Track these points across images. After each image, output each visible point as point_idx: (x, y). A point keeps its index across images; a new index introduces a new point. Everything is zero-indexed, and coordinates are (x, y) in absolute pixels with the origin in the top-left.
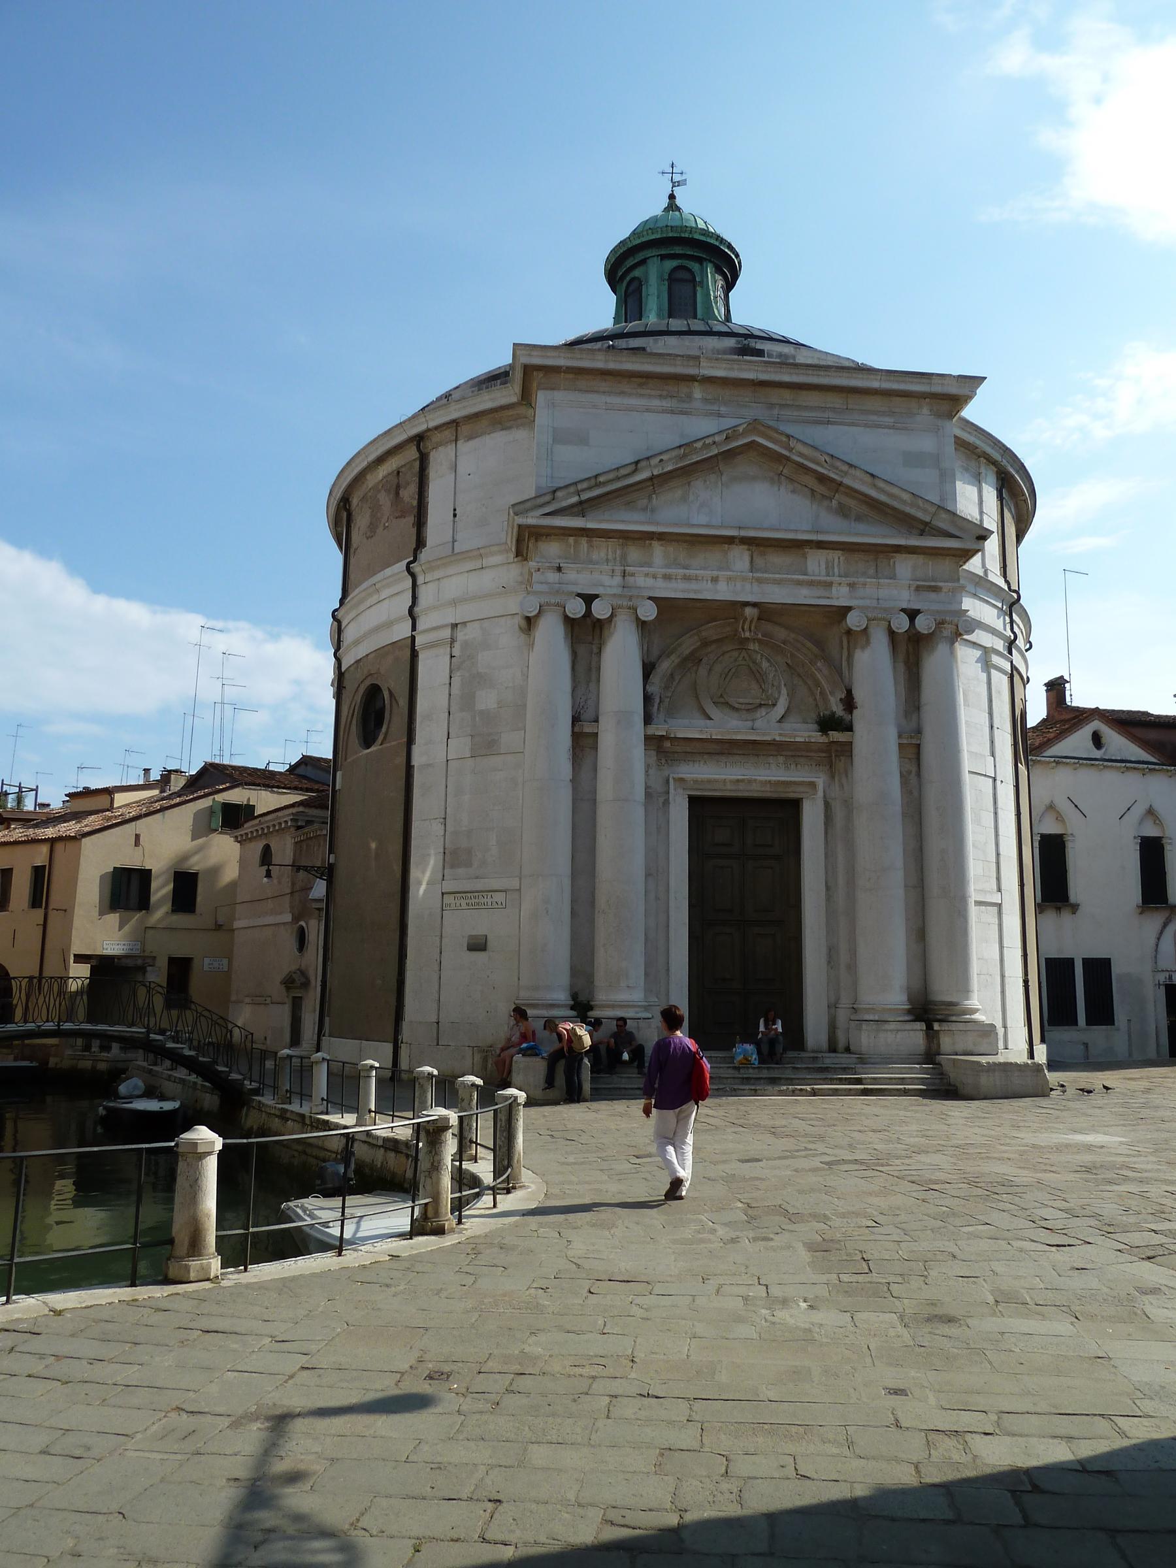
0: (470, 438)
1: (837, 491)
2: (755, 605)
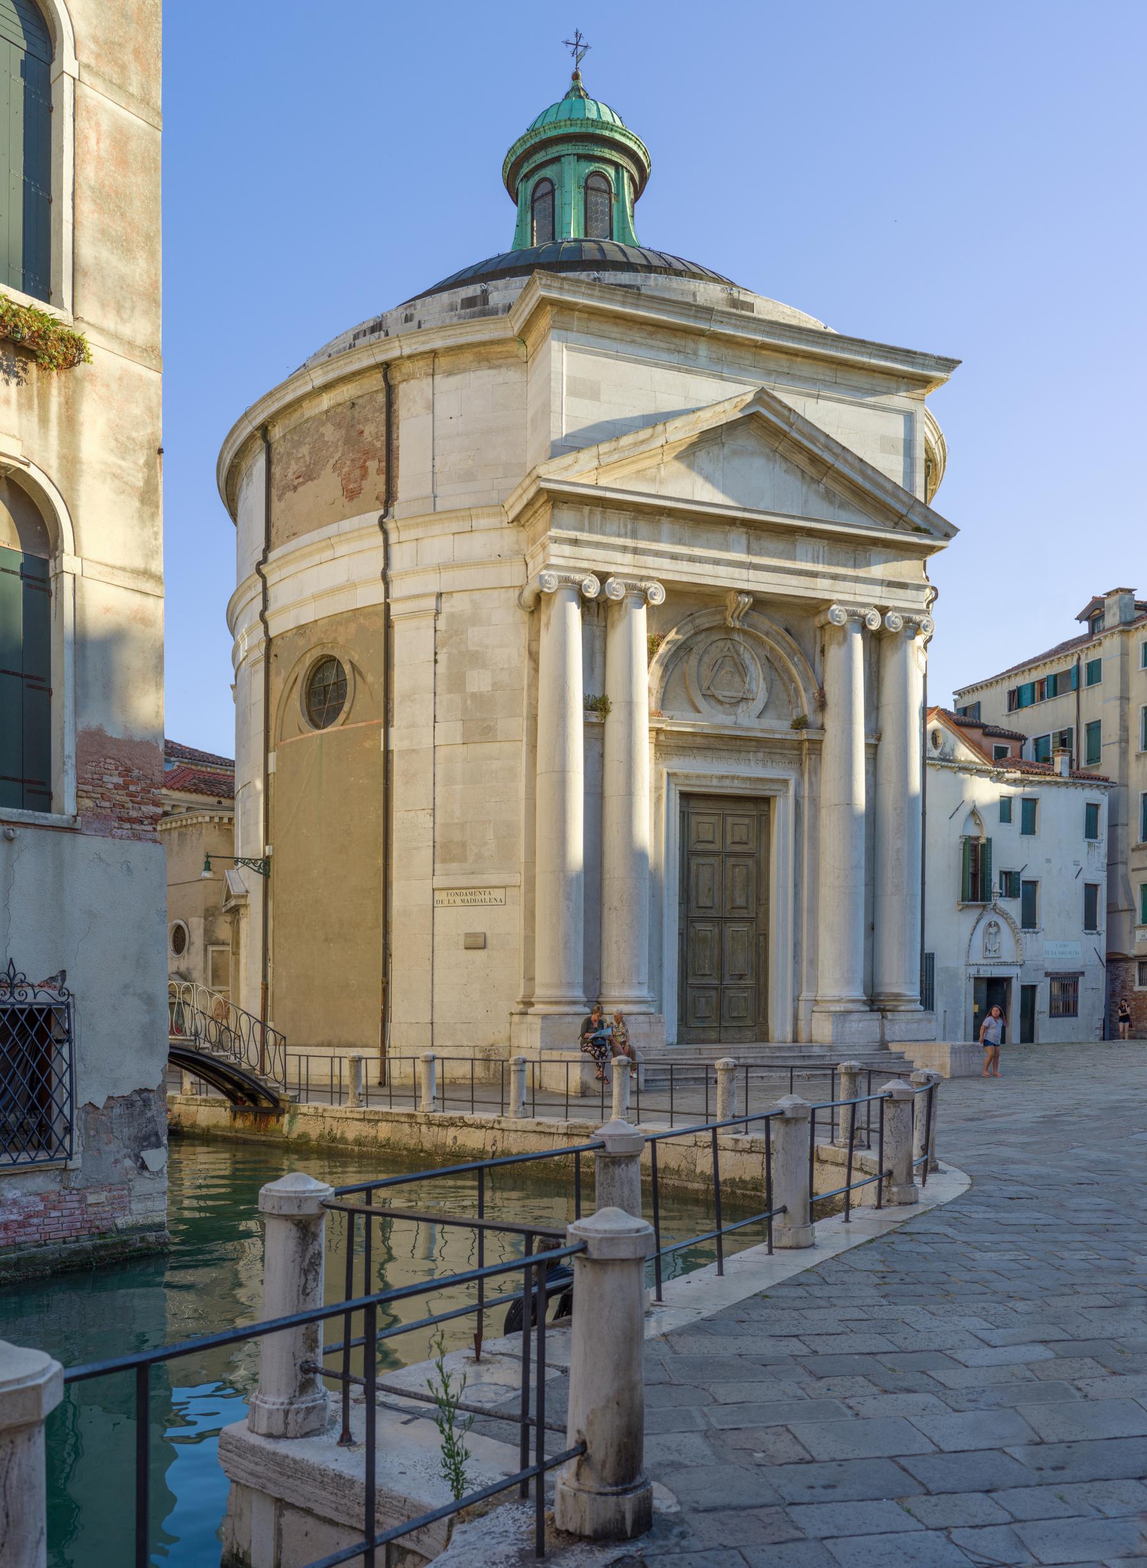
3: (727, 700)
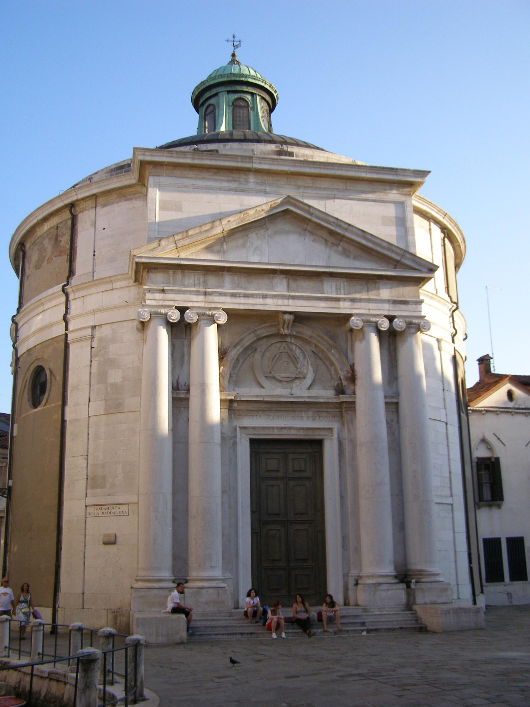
0: (104, 206)
1: (341, 241)
2: (290, 313)
3: (284, 379)
